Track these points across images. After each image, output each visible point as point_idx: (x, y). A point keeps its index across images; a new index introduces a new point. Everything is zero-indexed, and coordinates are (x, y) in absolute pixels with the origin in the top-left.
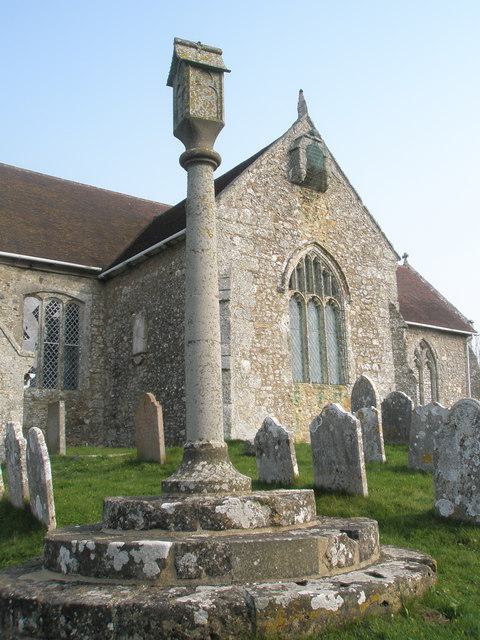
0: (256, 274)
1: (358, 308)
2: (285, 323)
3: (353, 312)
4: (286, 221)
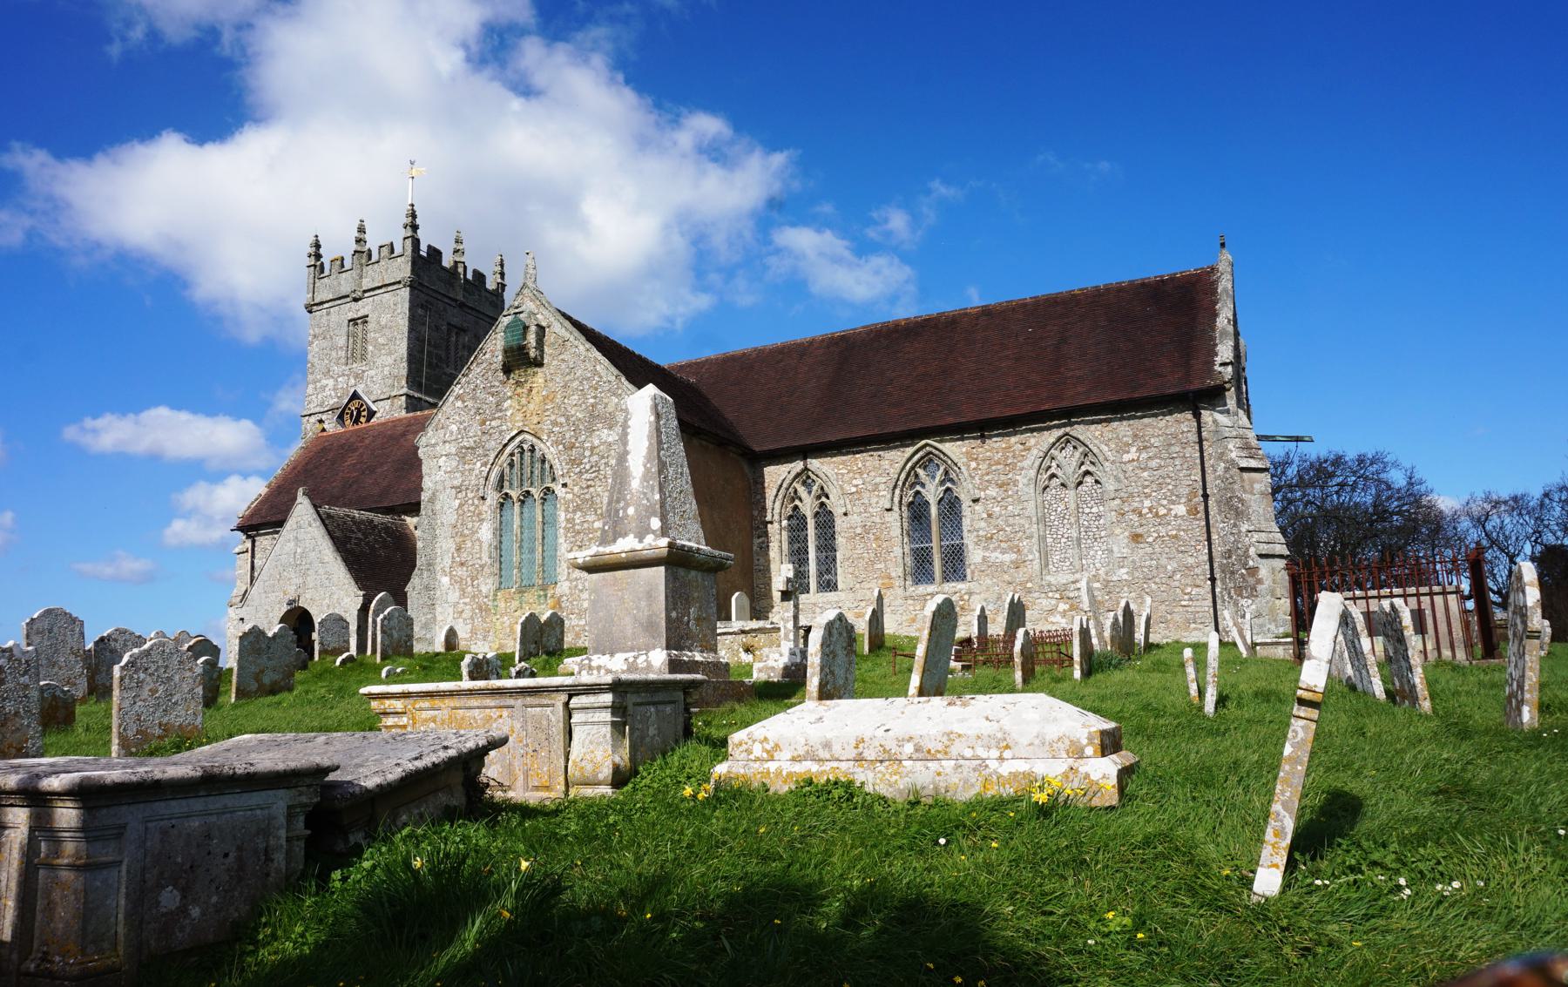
0: (458, 489)
1: (576, 489)
2: (486, 533)
3: (570, 496)
4: (495, 419)
